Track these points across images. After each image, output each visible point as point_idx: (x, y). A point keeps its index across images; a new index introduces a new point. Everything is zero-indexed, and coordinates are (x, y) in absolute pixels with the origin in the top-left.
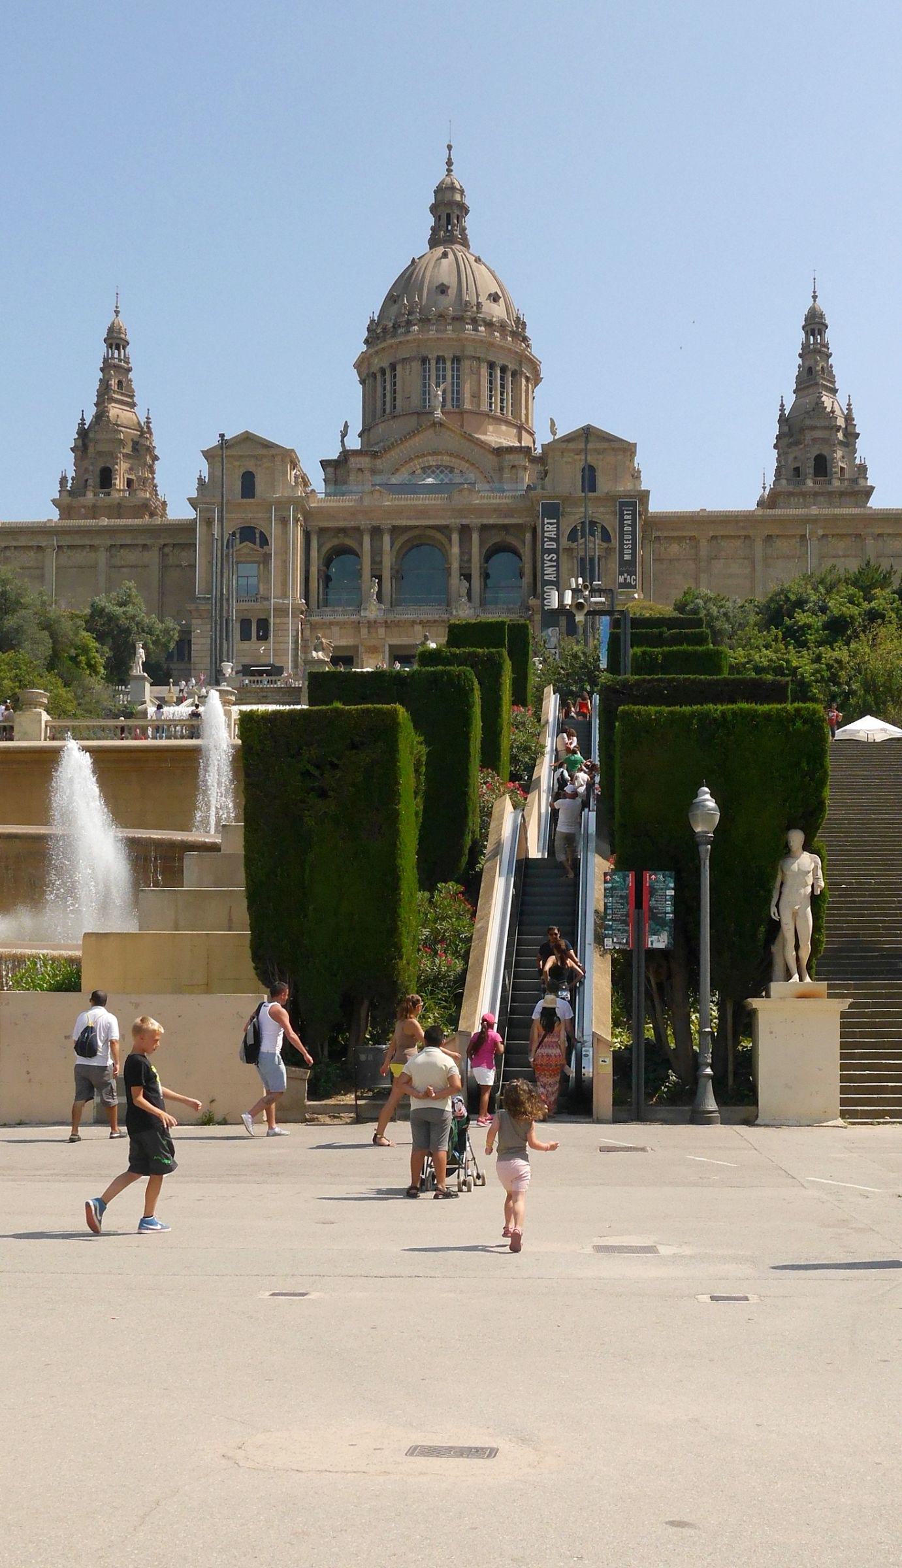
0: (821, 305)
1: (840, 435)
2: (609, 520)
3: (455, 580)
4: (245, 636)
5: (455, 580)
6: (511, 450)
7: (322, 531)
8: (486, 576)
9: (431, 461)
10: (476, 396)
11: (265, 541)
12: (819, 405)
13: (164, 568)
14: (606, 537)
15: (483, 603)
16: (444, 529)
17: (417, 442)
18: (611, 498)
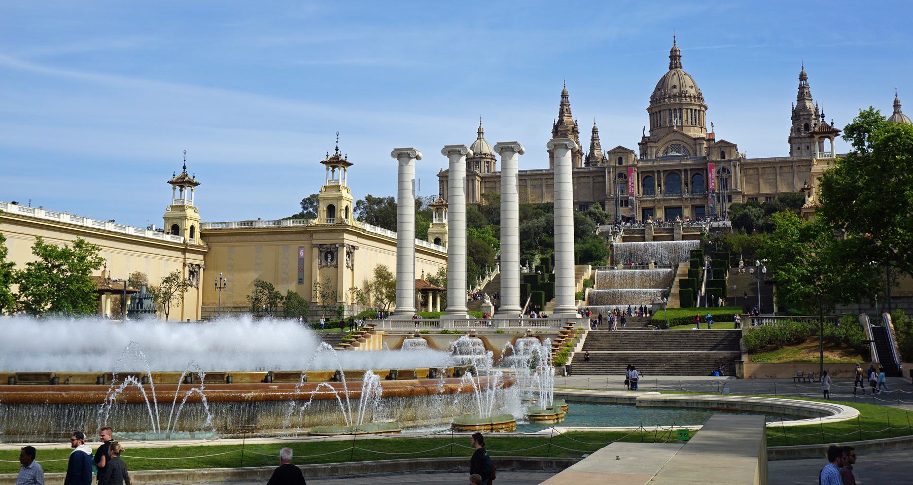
0: (806, 71)
1: (813, 116)
2: (728, 167)
3: (683, 186)
4: (622, 206)
5: (683, 186)
6: (699, 138)
7: (642, 172)
8: (692, 182)
9: (675, 142)
10: (687, 120)
11: (626, 177)
12: (805, 107)
13: (594, 183)
14: (729, 172)
15: (692, 192)
16: (679, 170)
17: (669, 137)
18: (730, 161)
